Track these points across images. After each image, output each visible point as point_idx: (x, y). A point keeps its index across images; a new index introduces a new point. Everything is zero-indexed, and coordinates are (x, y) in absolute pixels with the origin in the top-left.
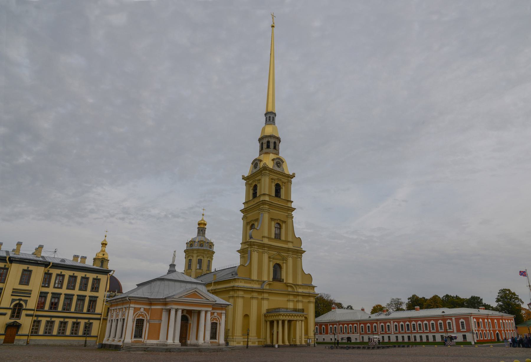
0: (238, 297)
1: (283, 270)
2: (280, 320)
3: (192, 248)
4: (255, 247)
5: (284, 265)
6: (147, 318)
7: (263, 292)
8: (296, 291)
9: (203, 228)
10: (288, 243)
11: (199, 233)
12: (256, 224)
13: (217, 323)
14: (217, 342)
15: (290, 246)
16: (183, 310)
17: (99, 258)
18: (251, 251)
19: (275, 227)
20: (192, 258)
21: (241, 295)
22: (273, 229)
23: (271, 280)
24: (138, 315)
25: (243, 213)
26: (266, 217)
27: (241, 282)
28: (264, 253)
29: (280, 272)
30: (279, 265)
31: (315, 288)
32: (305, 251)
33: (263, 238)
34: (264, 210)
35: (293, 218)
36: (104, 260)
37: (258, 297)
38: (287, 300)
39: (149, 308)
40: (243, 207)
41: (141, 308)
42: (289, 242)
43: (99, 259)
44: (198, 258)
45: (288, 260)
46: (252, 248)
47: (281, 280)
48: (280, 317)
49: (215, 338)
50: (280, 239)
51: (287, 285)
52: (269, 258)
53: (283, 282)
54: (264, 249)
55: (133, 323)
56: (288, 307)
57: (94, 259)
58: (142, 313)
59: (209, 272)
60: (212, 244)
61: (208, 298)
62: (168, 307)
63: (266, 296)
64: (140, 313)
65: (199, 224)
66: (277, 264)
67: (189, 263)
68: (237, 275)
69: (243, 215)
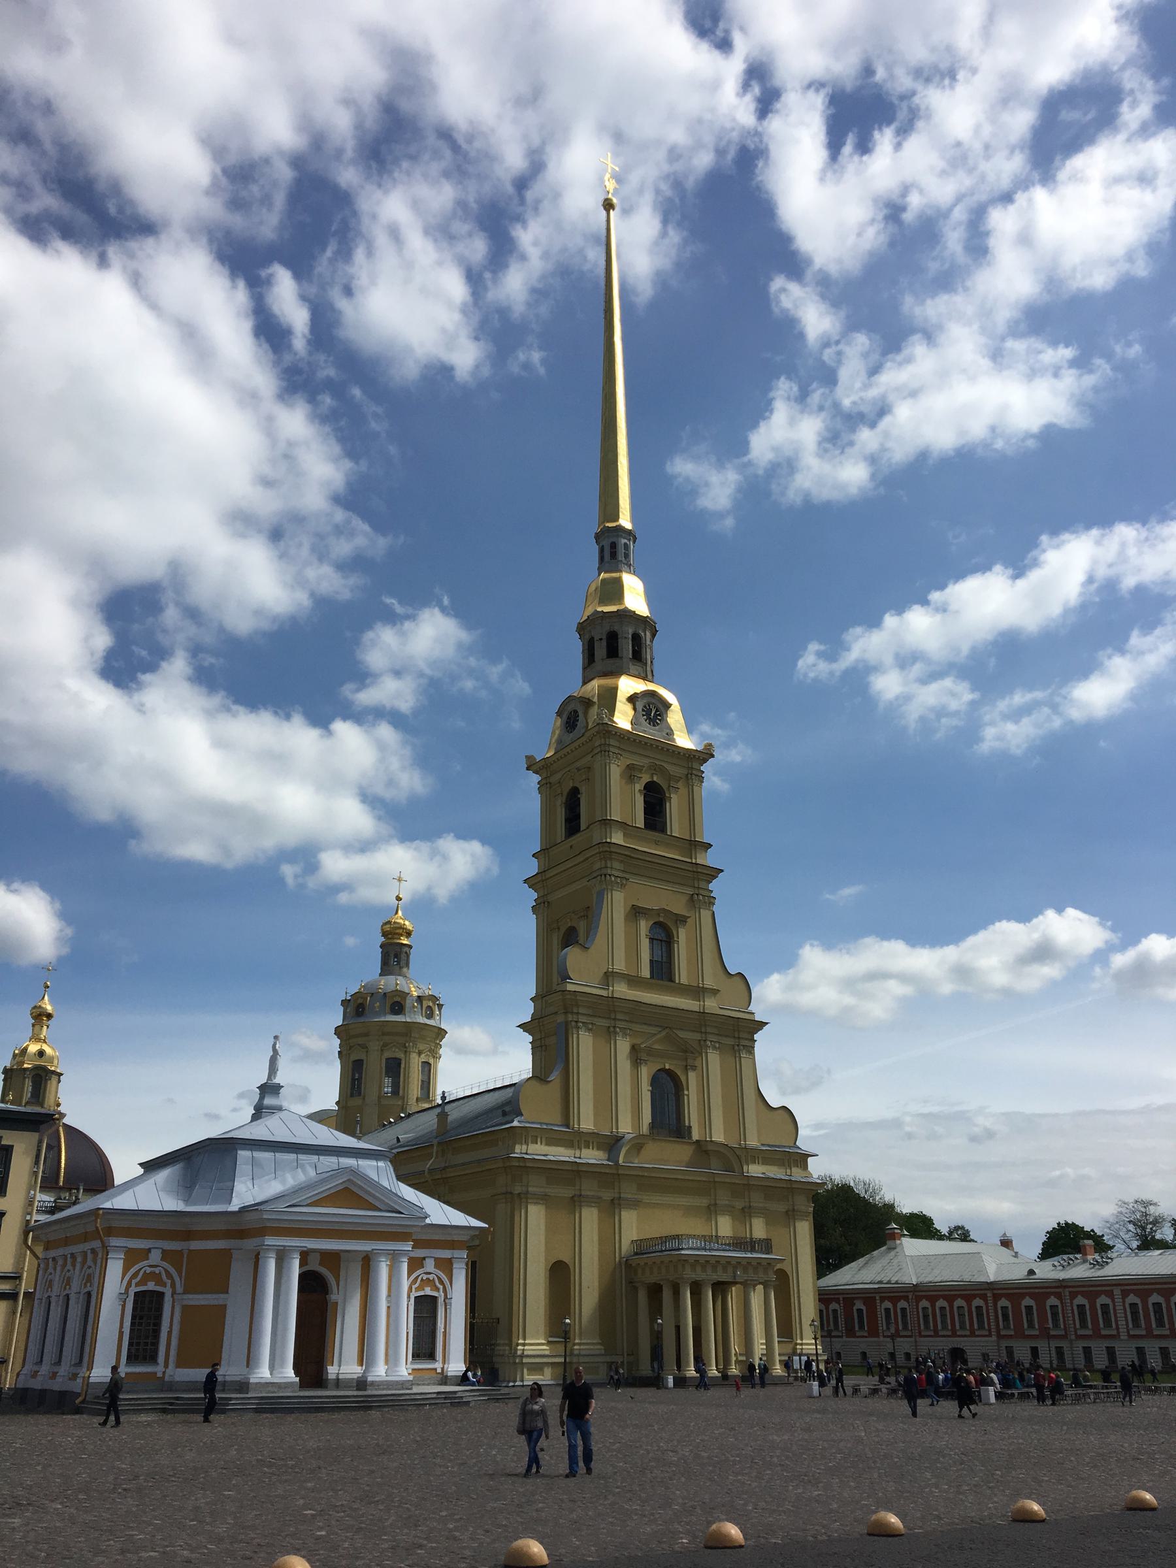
1: (688, 1095)
3: (362, 1020)
6: (173, 1285)
12: (582, 927)
13: (435, 1299)
14: (439, 1370)
15: (711, 1005)
16: (305, 1255)
18: (567, 1023)
19: (652, 940)
20: (363, 1057)
22: (645, 944)
23: (645, 1129)
24: (138, 1279)
26: (617, 903)
30: (670, 1073)
32: (762, 1025)
34: (608, 876)
36: (43, 1074)
38: (708, 1207)
39: (180, 1252)
40: (532, 867)
41: (149, 1250)
44: (387, 1054)
46: (570, 1015)
47: (680, 1131)
49: (431, 1356)
50: (671, 980)
52: (634, 1049)
53: (690, 1137)
55: (124, 1307)
57: (6, 1071)
58: (157, 1270)
59: (427, 1106)
60: (434, 1003)
61: (396, 1207)
62: (250, 1244)
64: (149, 1270)
65: (384, 934)
66: (662, 1070)
67: (353, 1075)
68: (522, 1115)
69: (535, 895)
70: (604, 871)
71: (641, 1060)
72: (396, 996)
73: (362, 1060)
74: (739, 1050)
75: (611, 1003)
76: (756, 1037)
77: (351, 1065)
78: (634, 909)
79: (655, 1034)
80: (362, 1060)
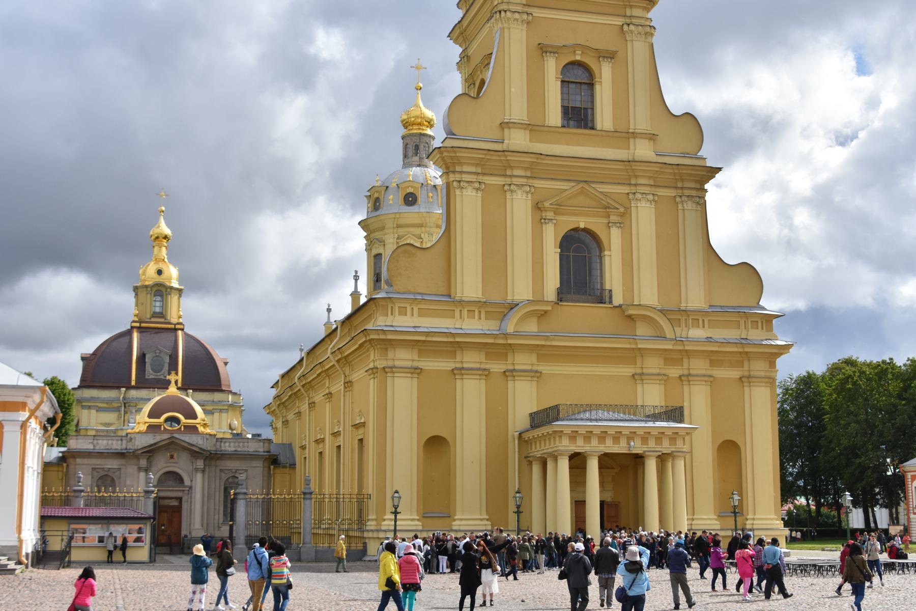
0: (394, 373)
2: (561, 455)
4: (466, 168)
5: (616, 233)
7: (513, 348)
8: (674, 337)
9: (421, 134)
10: (632, 141)
11: (405, 156)
15: (643, 150)
17: (147, 283)
19: (563, 82)
20: (381, 251)
21: (409, 364)
25: (461, 46)
27: (403, 311)
28: (512, 191)
29: (601, 263)
31: (774, 321)
33: (506, 131)
34: (503, 13)
35: (652, 35)
36: (163, 290)
37: (487, 366)
42: (634, 135)
43: (146, 287)
45: (633, 210)
48: (560, 442)
50: (593, 128)
51: (626, 313)
52: (538, 207)
53: (611, 302)
54: (509, 172)
56: (639, 403)
63: (522, 361)
65: (406, 124)
66: (576, 230)
70: (501, 7)
71: (545, 219)
72: (408, 187)
73: (381, 254)
74: (682, 202)
75: (502, 158)
76: (707, 186)
77: (372, 258)
78: (541, 48)
79: (567, 190)
80: (381, 254)
